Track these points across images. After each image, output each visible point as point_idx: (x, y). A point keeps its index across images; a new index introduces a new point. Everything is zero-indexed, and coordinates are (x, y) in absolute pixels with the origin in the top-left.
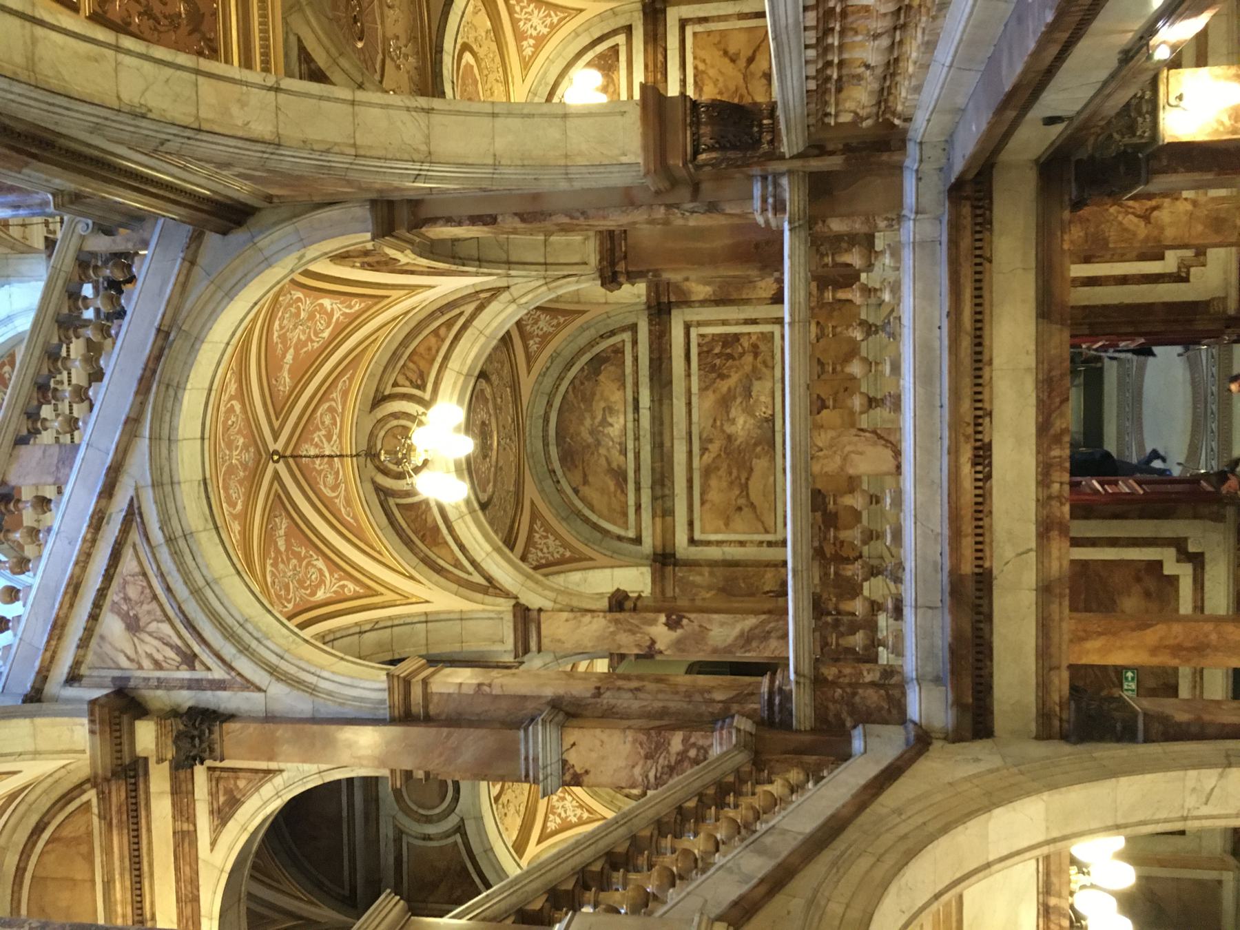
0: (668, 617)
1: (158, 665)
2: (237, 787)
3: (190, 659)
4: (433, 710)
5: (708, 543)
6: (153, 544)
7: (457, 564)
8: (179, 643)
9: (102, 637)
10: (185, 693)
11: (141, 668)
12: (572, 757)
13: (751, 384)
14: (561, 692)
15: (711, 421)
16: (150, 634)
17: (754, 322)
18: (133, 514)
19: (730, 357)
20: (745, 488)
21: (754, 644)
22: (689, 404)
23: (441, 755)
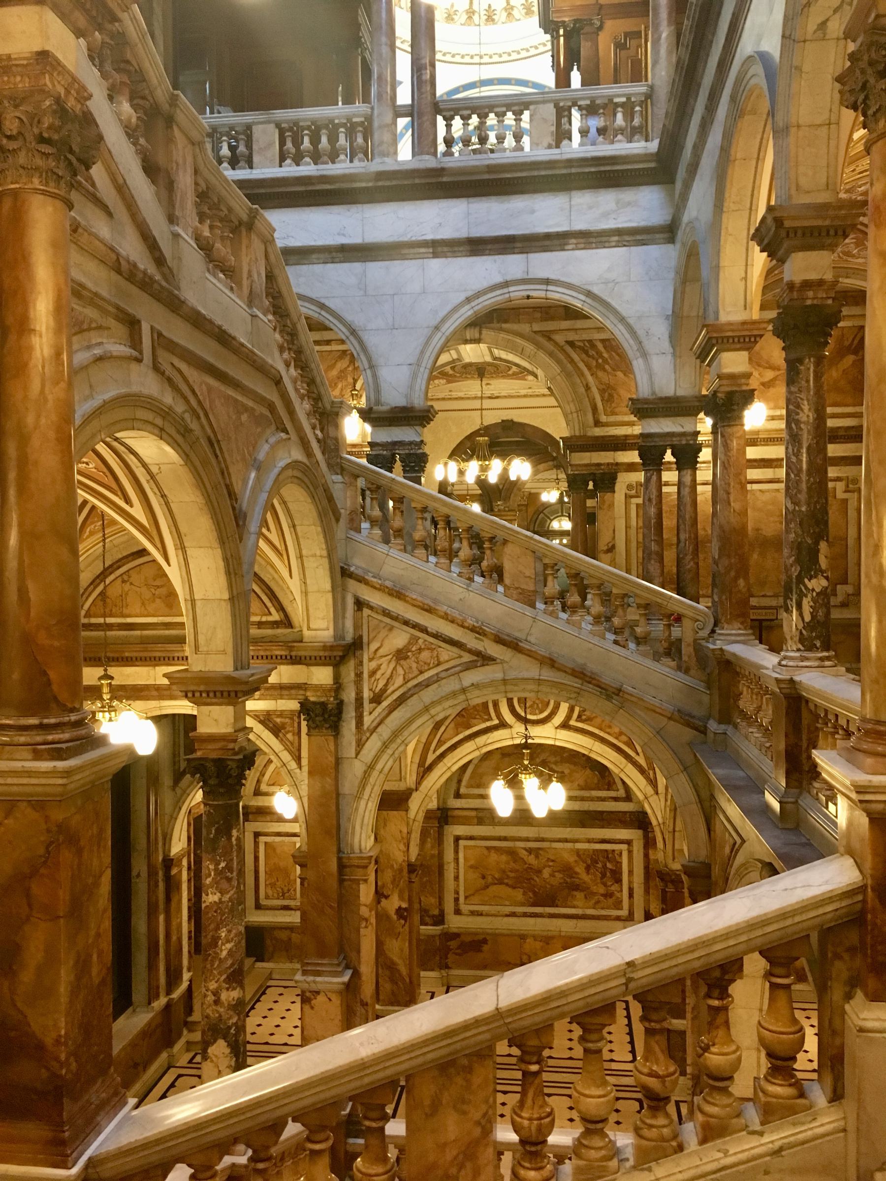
0: (405, 909)
1: (373, 673)
2: (287, 732)
3: (377, 699)
4: (346, 883)
5: (456, 852)
7: (440, 743)
8: (389, 691)
9: (391, 628)
10: (353, 695)
11: (371, 660)
12: (321, 998)
13: (582, 891)
14: (364, 978)
15: (552, 858)
16: (395, 668)
17: (631, 896)
18: (484, 659)
19: (604, 875)
20: (500, 882)
21: (388, 973)
22: (566, 841)
23: (319, 901)
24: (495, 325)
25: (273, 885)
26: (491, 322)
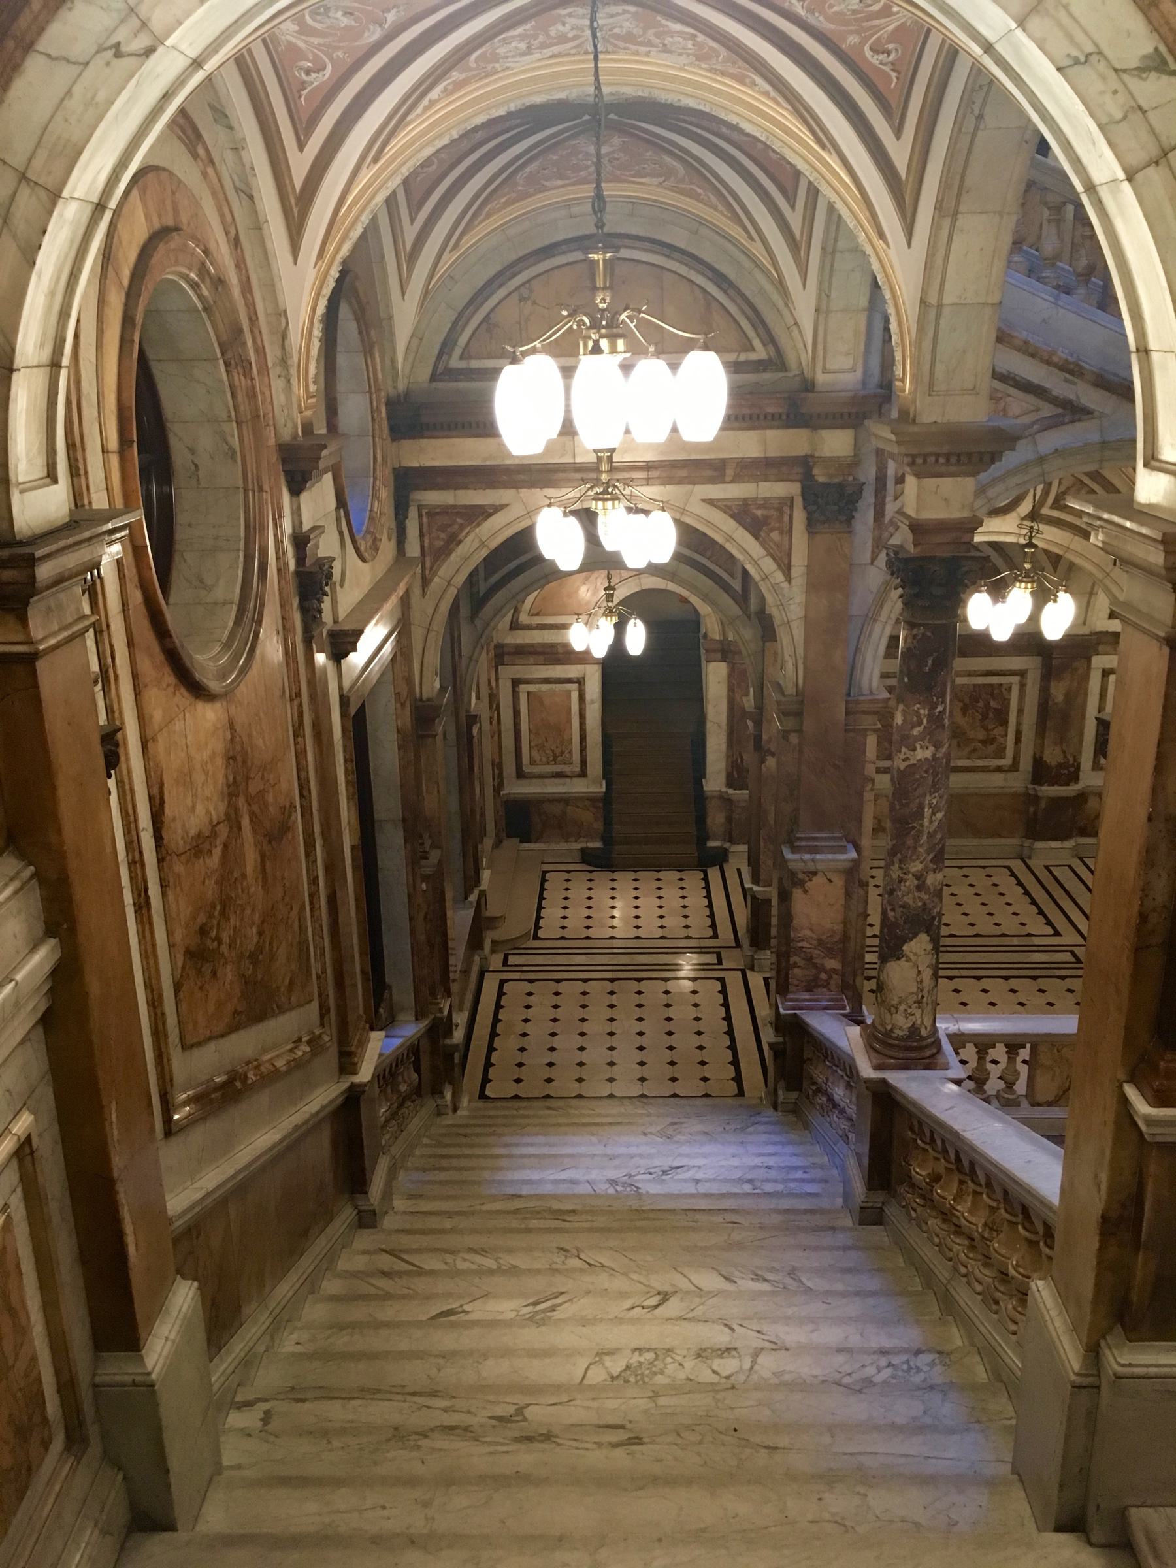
2: (772, 530)
6: (1037, 437)
12: (818, 880)
17: (1018, 740)
18: (1073, 411)
19: (985, 717)
25: (540, 748)
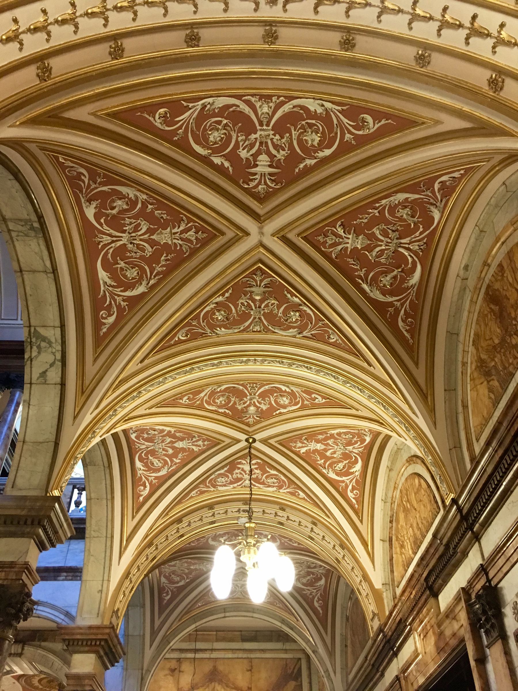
24: (37, 643)
26: (34, 640)
